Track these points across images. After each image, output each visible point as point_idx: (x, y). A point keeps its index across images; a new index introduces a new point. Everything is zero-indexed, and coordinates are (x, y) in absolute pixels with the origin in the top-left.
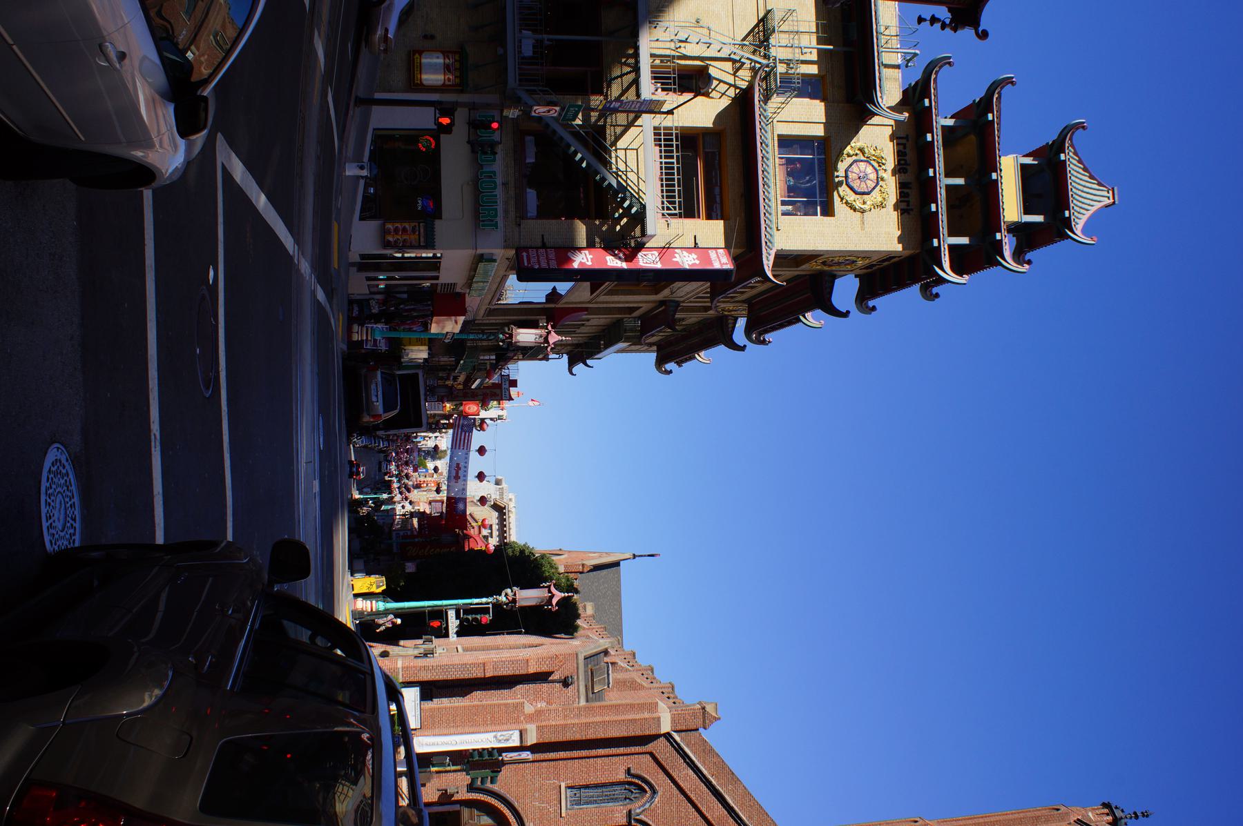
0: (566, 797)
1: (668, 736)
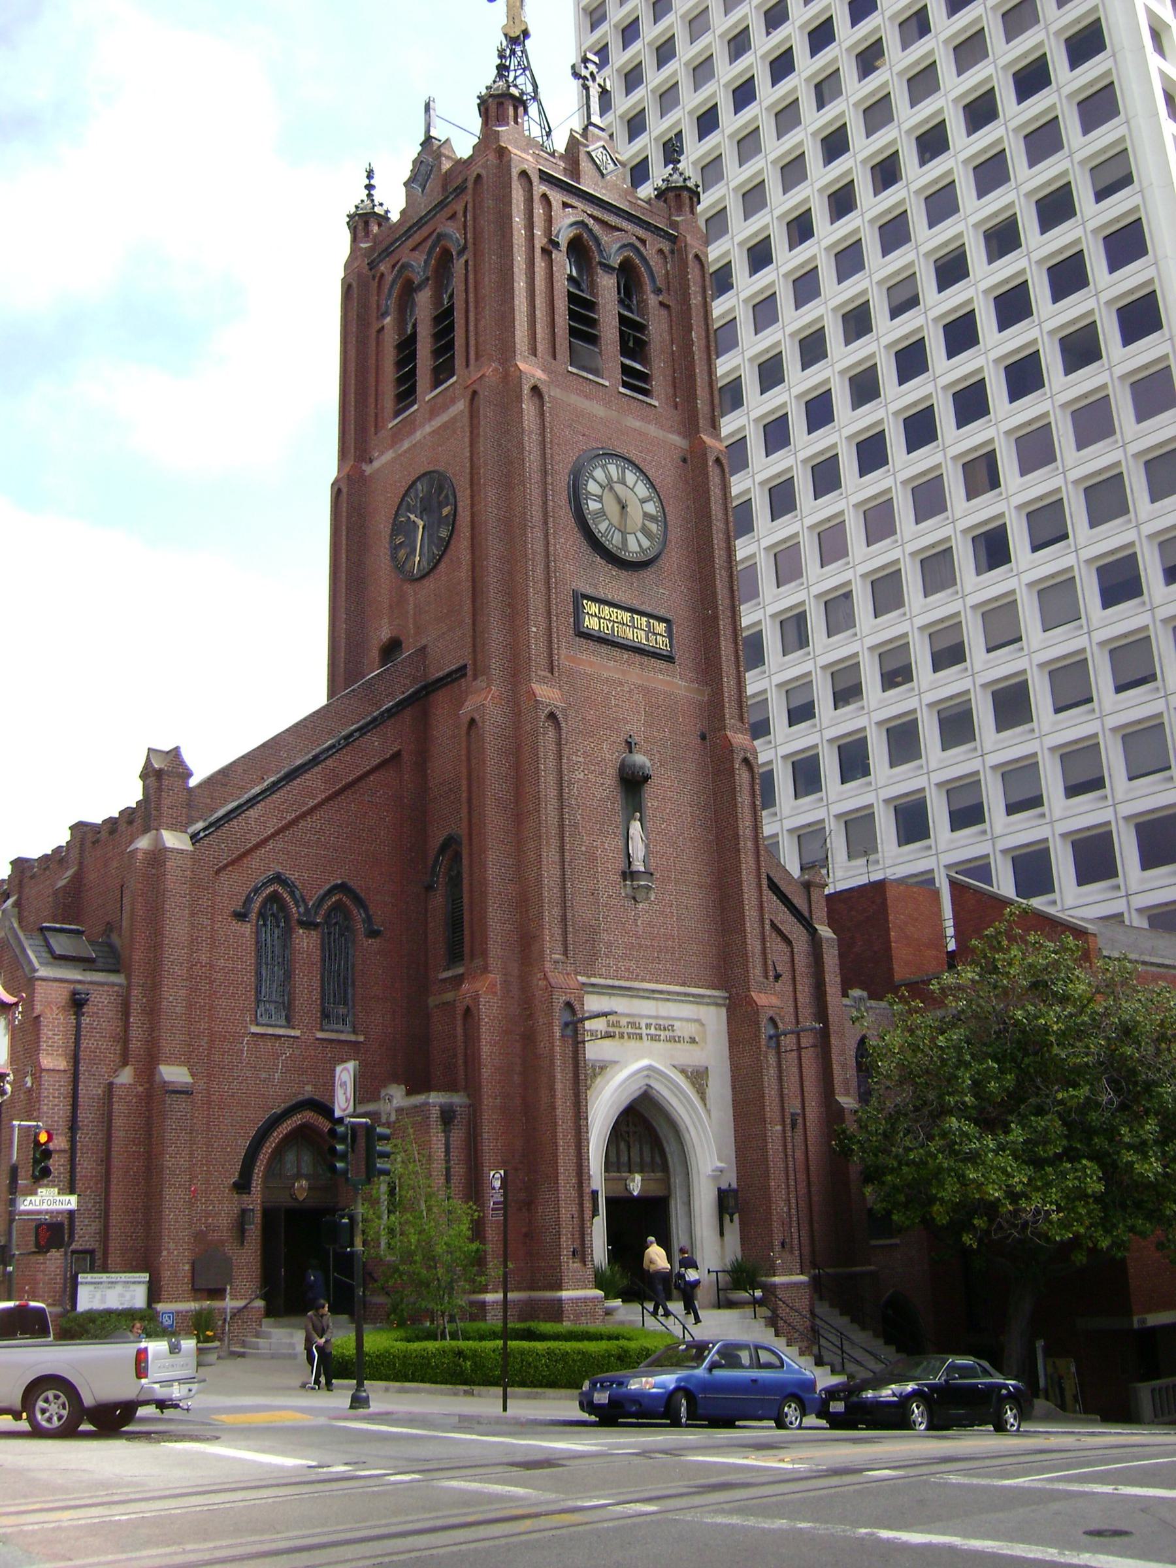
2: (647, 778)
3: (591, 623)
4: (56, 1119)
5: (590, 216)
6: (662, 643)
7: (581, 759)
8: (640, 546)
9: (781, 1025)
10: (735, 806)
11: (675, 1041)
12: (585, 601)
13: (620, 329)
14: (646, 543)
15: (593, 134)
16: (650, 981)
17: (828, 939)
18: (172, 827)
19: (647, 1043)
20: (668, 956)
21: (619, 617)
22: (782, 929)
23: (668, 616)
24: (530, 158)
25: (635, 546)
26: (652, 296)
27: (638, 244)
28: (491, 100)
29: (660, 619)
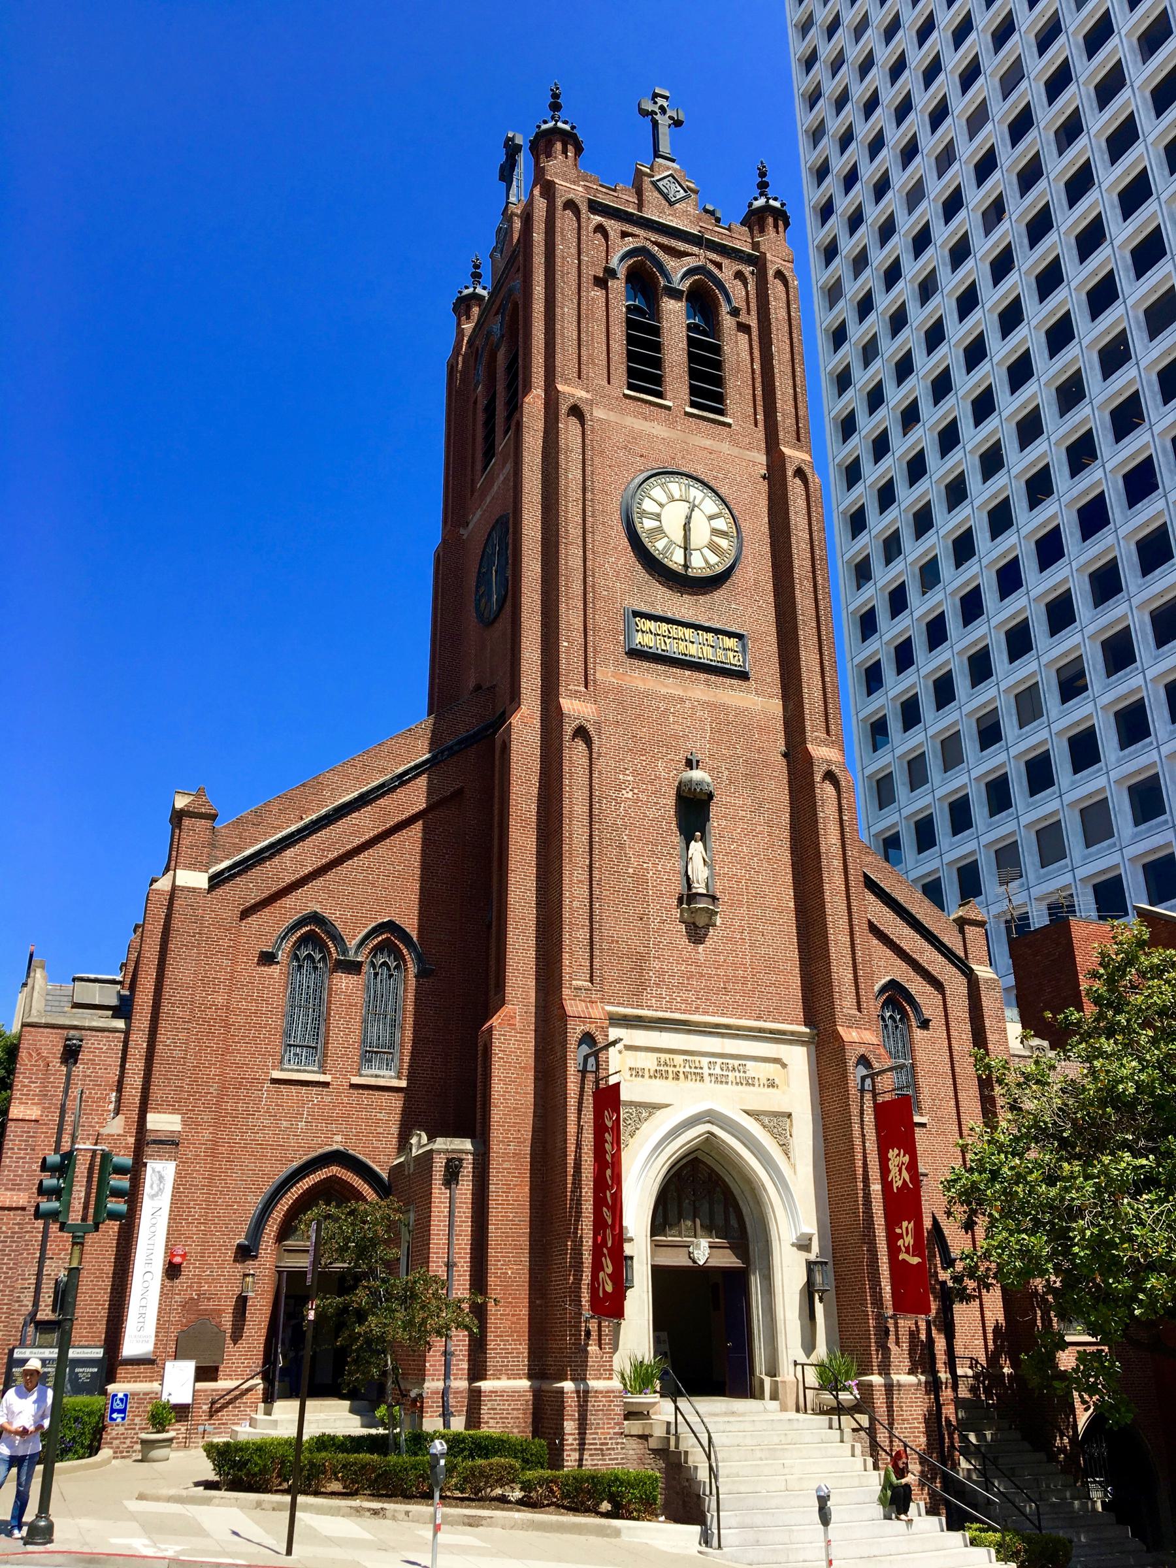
0: (298, 1071)
1: (216, 881)
2: (711, 796)
3: (643, 640)
4: (20, 1172)
5: (655, 243)
6: (733, 660)
7: (629, 778)
8: (706, 562)
9: (876, 1065)
10: (816, 821)
11: (748, 1084)
13: (689, 351)
14: (713, 559)
15: (660, 165)
16: (713, 1014)
17: (987, 980)
18: (192, 866)
19: (708, 1085)
20: (739, 987)
22: (930, 969)
23: (741, 632)
24: (580, 189)
25: (701, 563)
26: (728, 317)
29: (731, 635)
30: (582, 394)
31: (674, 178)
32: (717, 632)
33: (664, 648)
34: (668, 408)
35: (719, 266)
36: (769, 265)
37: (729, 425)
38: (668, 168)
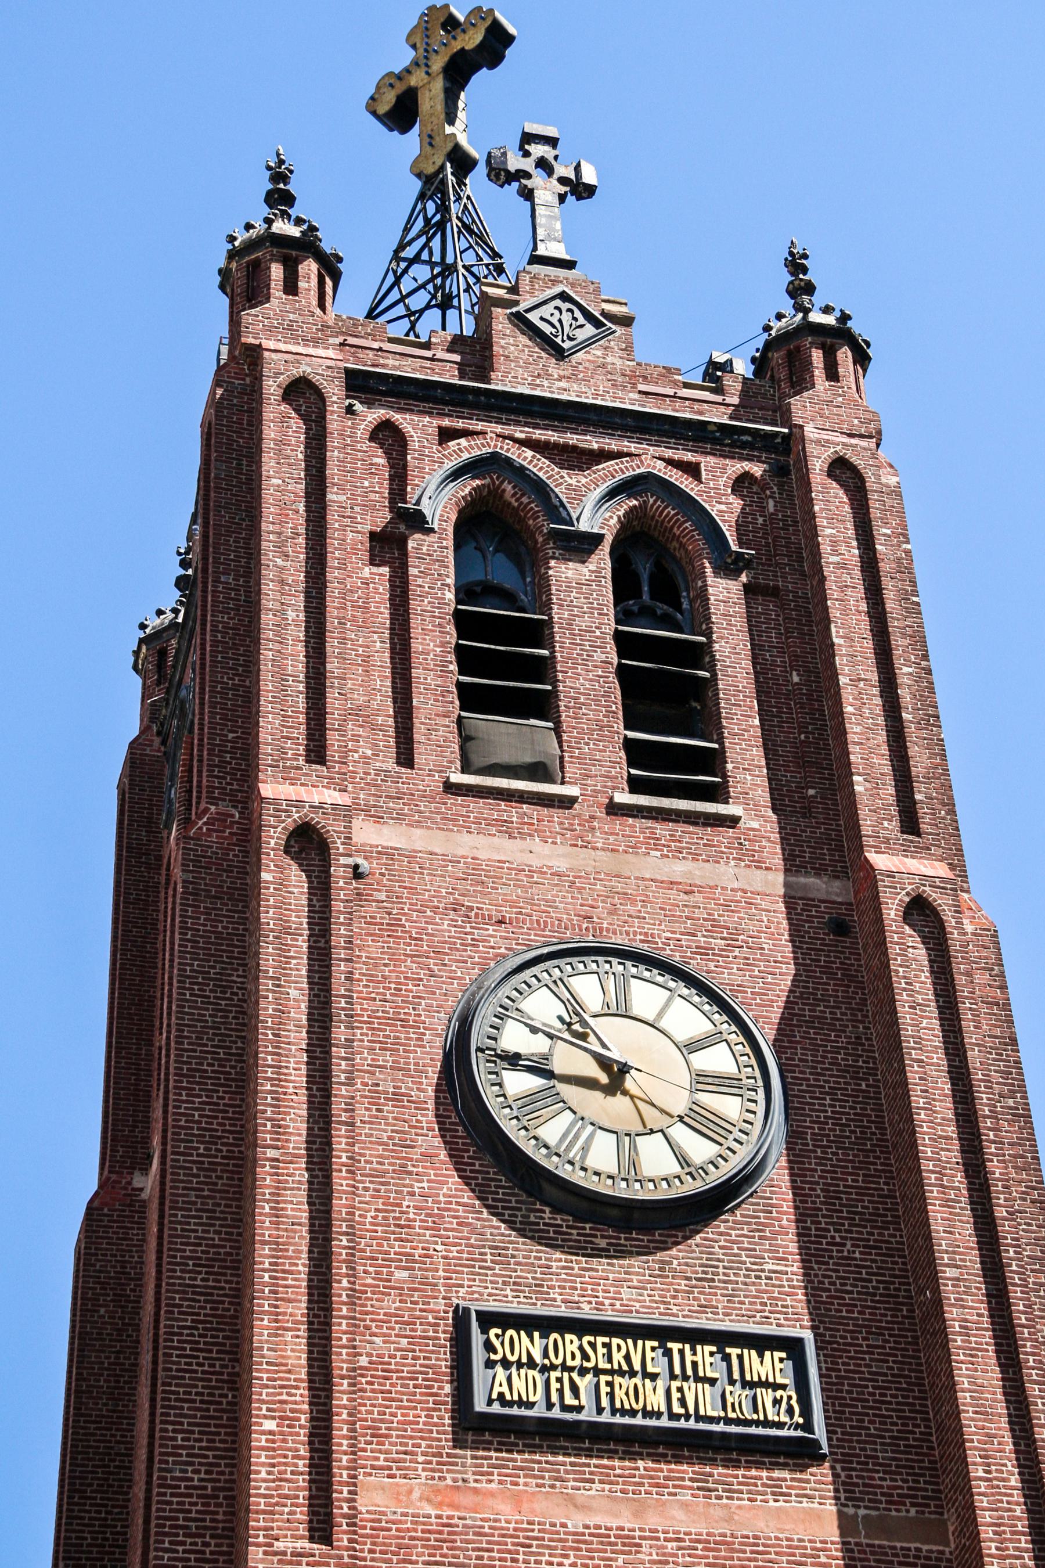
8: (683, 1160)
12: (494, 1331)
14: (700, 1150)
15: (535, 278)
21: (618, 1357)
27: (675, 476)
28: (234, 265)
29: (761, 1343)
30: (331, 796)
31: (564, 297)
32: (721, 1339)
33: (569, 1400)
34: (567, 803)
35: (692, 470)
36: (810, 448)
37: (733, 821)
38: (555, 282)
